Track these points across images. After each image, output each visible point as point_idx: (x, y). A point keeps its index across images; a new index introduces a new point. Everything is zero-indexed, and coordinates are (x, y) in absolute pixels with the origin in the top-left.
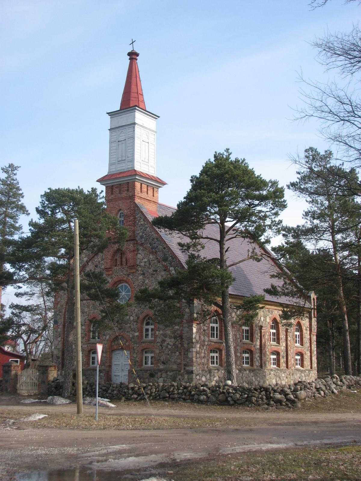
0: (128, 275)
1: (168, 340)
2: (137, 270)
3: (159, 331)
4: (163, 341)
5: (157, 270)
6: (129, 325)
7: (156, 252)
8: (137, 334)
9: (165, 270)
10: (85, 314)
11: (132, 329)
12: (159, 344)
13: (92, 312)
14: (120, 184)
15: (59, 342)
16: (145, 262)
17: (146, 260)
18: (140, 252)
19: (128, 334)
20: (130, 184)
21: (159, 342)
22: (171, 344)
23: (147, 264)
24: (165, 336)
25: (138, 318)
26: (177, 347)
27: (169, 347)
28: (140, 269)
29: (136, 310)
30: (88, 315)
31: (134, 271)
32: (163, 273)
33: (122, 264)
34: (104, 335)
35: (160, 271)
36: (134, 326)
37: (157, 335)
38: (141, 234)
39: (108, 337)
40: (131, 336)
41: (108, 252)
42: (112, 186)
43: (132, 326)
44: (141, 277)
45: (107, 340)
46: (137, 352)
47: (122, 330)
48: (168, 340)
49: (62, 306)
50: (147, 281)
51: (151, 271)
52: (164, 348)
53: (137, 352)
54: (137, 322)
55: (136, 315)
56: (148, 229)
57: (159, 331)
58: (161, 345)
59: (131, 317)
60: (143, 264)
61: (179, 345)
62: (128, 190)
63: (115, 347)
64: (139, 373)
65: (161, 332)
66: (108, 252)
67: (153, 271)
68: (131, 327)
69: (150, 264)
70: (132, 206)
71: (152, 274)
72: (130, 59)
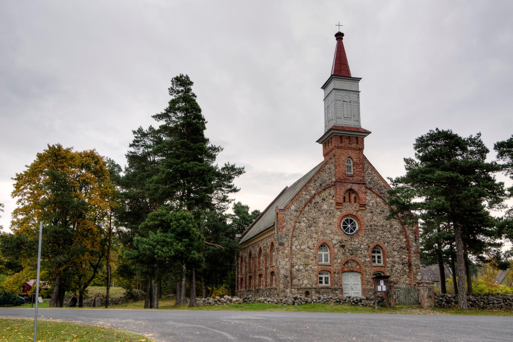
0: (357, 211)
1: (397, 266)
10: (313, 239)
12: (389, 269)
13: (321, 238)
14: (349, 137)
15: (287, 262)
16: (373, 203)
17: (373, 201)
18: (368, 194)
19: (360, 259)
20: (359, 139)
22: (400, 268)
23: (375, 205)
24: (394, 262)
25: (369, 247)
26: (405, 271)
27: (398, 271)
28: (368, 208)
31: (364, 208)
33: (350, 201)
36: (366, 253)
38: (369, 180)
39: (339, 261)
40: (363, 261)
41: (340, 190)
42: (341, 137)
44: (370, 214)
45: (339, 263)
47: (353, 256)
48: (397, 266)
49: (289, 230)
52: (394, 272)
55: (367, 244)
56: (376, 178)
60: (371, 204)
61: (407, 270)
62: (357, 143)
63: (346, 269)
66: (340, 190)
70: (361, 157)
71: (380, 213)
72: (337, 39)
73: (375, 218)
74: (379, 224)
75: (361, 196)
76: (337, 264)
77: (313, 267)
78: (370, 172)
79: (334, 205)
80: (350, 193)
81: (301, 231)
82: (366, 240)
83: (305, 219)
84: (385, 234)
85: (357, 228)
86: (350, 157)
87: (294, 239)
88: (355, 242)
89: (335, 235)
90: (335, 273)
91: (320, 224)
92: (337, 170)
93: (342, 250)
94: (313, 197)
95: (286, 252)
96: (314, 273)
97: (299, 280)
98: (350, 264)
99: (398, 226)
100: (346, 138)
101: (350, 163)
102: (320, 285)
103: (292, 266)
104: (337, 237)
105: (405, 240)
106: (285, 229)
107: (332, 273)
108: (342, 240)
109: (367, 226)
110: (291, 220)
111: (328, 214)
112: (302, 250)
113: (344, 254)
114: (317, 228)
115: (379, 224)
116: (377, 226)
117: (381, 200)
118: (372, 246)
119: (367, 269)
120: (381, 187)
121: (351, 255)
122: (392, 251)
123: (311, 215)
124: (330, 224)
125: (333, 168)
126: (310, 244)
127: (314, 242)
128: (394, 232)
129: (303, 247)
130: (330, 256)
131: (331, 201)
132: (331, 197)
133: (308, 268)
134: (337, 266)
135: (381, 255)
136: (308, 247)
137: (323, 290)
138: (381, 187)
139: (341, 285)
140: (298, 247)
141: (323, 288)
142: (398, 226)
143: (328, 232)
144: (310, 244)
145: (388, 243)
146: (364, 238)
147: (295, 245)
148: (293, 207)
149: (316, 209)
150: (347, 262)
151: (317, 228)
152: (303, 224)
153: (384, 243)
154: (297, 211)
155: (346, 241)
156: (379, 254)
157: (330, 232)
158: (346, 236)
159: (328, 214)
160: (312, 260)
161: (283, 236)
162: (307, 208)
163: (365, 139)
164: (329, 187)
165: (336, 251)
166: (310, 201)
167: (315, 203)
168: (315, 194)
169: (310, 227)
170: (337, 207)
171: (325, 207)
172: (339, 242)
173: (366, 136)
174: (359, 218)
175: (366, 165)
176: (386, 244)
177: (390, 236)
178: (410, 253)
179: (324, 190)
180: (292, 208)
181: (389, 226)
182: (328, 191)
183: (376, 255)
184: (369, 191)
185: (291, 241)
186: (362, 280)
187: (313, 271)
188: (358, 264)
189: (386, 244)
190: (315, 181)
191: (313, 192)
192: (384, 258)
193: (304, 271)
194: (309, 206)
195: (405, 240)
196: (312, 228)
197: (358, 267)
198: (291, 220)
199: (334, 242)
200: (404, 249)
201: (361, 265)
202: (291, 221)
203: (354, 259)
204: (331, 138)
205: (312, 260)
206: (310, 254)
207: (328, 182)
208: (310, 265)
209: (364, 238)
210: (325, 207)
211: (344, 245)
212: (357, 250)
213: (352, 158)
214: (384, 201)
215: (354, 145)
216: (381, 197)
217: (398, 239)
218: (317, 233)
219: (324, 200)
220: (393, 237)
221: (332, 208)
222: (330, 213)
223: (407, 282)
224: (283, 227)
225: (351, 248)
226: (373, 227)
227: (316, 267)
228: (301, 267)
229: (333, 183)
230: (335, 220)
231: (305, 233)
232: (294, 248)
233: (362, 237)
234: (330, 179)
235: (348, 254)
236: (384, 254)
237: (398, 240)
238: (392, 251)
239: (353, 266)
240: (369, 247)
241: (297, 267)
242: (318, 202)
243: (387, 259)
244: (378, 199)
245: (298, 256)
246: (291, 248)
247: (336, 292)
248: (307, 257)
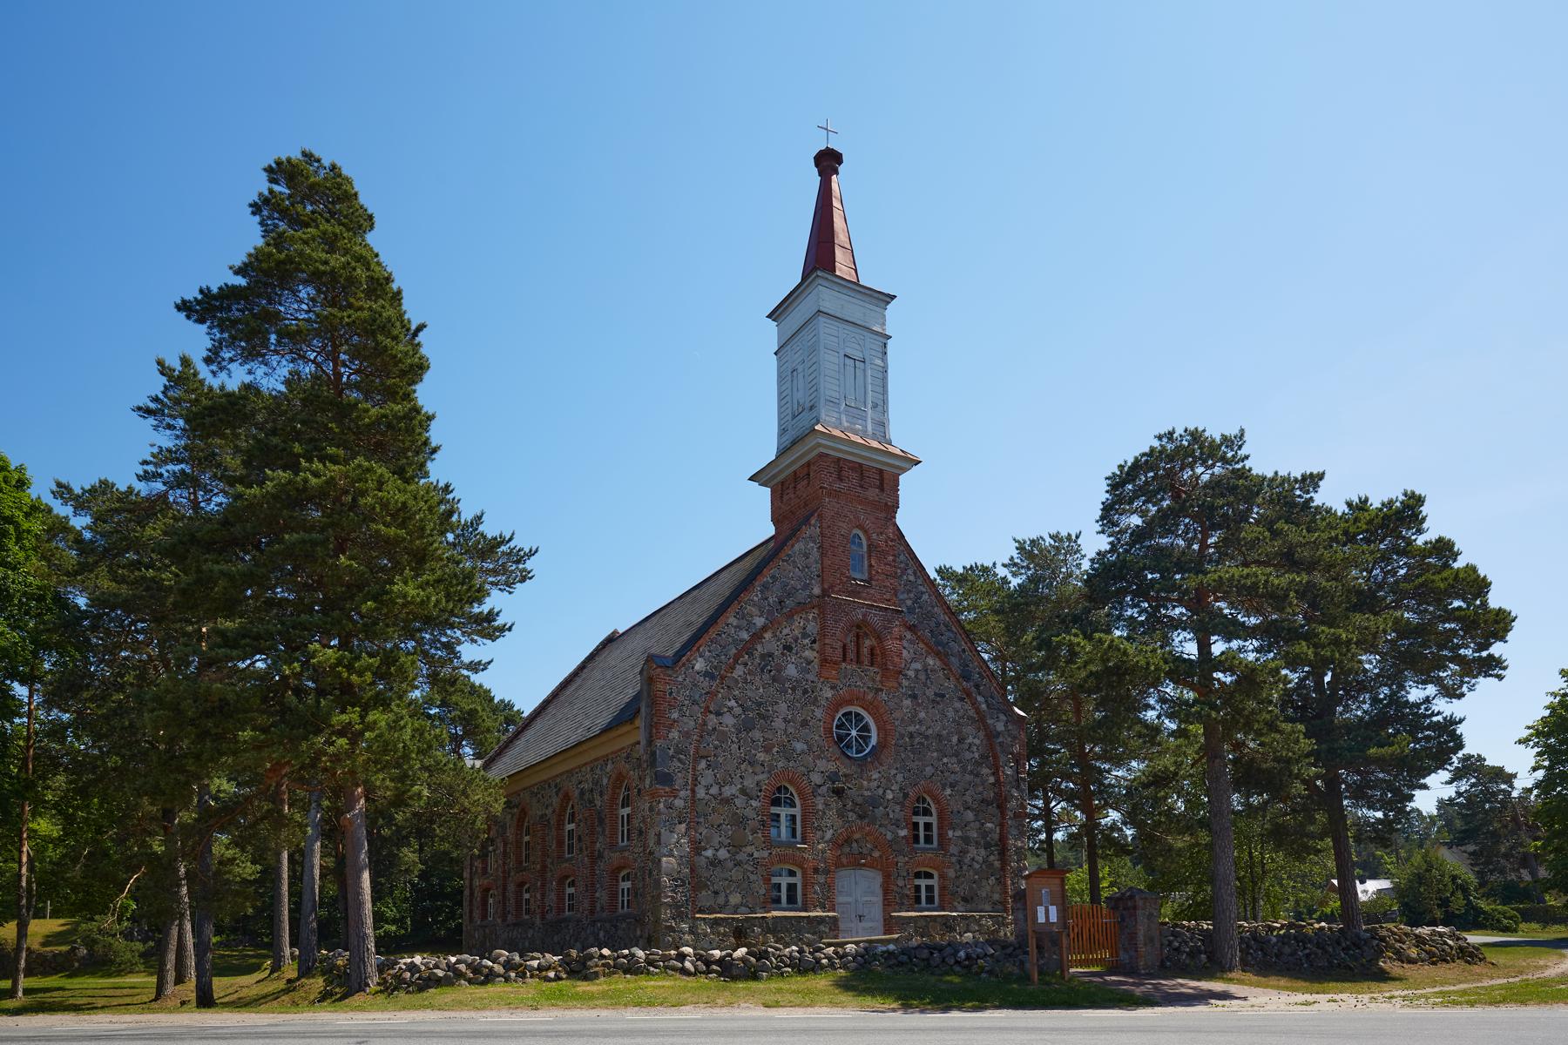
1: (973, 852)
2: (900, 684)
4: (963, 852)
5: (943, 696)
7: (947, 655)
8: (903, 833)
9: (962, 699)
12: (954, 859)
13: (780, 764)
16: (917, 671)
17: (918, 666)
23: (922, 677)
24: (966, 840)
25: (906, 796)
29: (900, 778)
32: (958, 705)
33: (859, 661)
34: (819, 828)
35: (951, 699)
36: (896, 812)
40: (889, 836)
42: (839, 459)
44: (908, 702)
48: (973, 852)
49: (687, 735)
50: (922, 715)
51: (930, 693)
54: (902, 804)
56: (925, 597)
60: (911, 673)
61: (997, 864)
65: (958, 833)
69: (928, 678)
73: (922, 715)
74: (930, 732)
75: (891, 645)
78: (912, 578)
79: (816, 664)
80: (858, 636)
81: (723, 737)
83: (733, 703)
85: (874, 741)
86: (861, 527)
87: (703, 764)
88: (870, 780)
89: (819, 757)
91: (778, 723)
92: (827, 562)
93: (835, 803)
94: (757, 636)
95: (679, 803)
97: (716, 893)
98: (855, 845)
99: (977, 742)
100: (852, 469)
101: (860, 545)
103: (697, 848)
104: (821, 765)
105: (992, 779)
106: (674, 734)
107: (810, 872)
108: (836, 774)
109: (902, 736)
110: (694, 702)
111: (799, 692)
112: (727, 801)
113: (841, 815)
115: (930, 732)
116: (927, 737)
120: (938, 624)
124: (805, 723)
125: (815, 554)
127: (761, 777)
128: (968, 755)
129: (728, 791)
130: (803, 821)
131: (807, 653)
132: (807, 641)
133: (742, 856)
138: (938, 624)
140: (714, 790)
142: (977, 742)
143: (799, 746)
144: (749, 783)
145: (952, 786)
147: (703, 783)
148: (699, 665)
149: (766, 676)
150: (848, 841)
152: (729, 720)
154: (712, 677)
156: (927, 819)
160: (754, 832)
161: (671, 752)
162: (739, 671)
163: (901, 478)
164: (802, 607)
166: (748, 648)
167: (763, 656)
168: (764, 629)
169: (749, 729)
171: (791, 671)
173: (905, 470)
175: (902, 558)
176: (948, 791)
178: (1003, 814)
179: (790, 616)
180: (697, 667)
181: (955, 739)
182: (798, 622)
183: (922, 820)
184: (909, 635)
185: (694, 769)
186: (886, 892)
187: (757, 863)
189: (948, 791)
190: (765, 587)
191: (760, 622)
192: (940, 828)
193: (730, 864)
195: (992, 779)
196: (756, 734)
198: (694, 702)
199: (816, 778)
200: (989, 803)
202: (696, 707)
204: (808, 464)
205: (754, 832)
206: (749, 813)
207: (802, 596)
208: (749, 849)
209: (893, 772)
210: (791, 671)
212: (874, 802)
213: (866, 532)
214: (946, 665)
215: (872, 493)
216: (937, 654)
217: (977, 775)
218: (767, 750)
219: (788, 648)
220: (964, 769)
221: (811, 677)
222: (805, 692)
223: (996, 897)
224: (671, 726)
225: (859, 800)
227: (765, 854)
228: (723, 854)
229: (815, 601)
232: (701, 793)
234: (806, 587)
235: (852, 816)
236: (940, 818)
237: (978, 780)
240: (906, 796)
241: (709, 853)
242: (771, 655)
243: (950, 833)
245: (716, 819)
246: (693, 791)
248: (740, 821)
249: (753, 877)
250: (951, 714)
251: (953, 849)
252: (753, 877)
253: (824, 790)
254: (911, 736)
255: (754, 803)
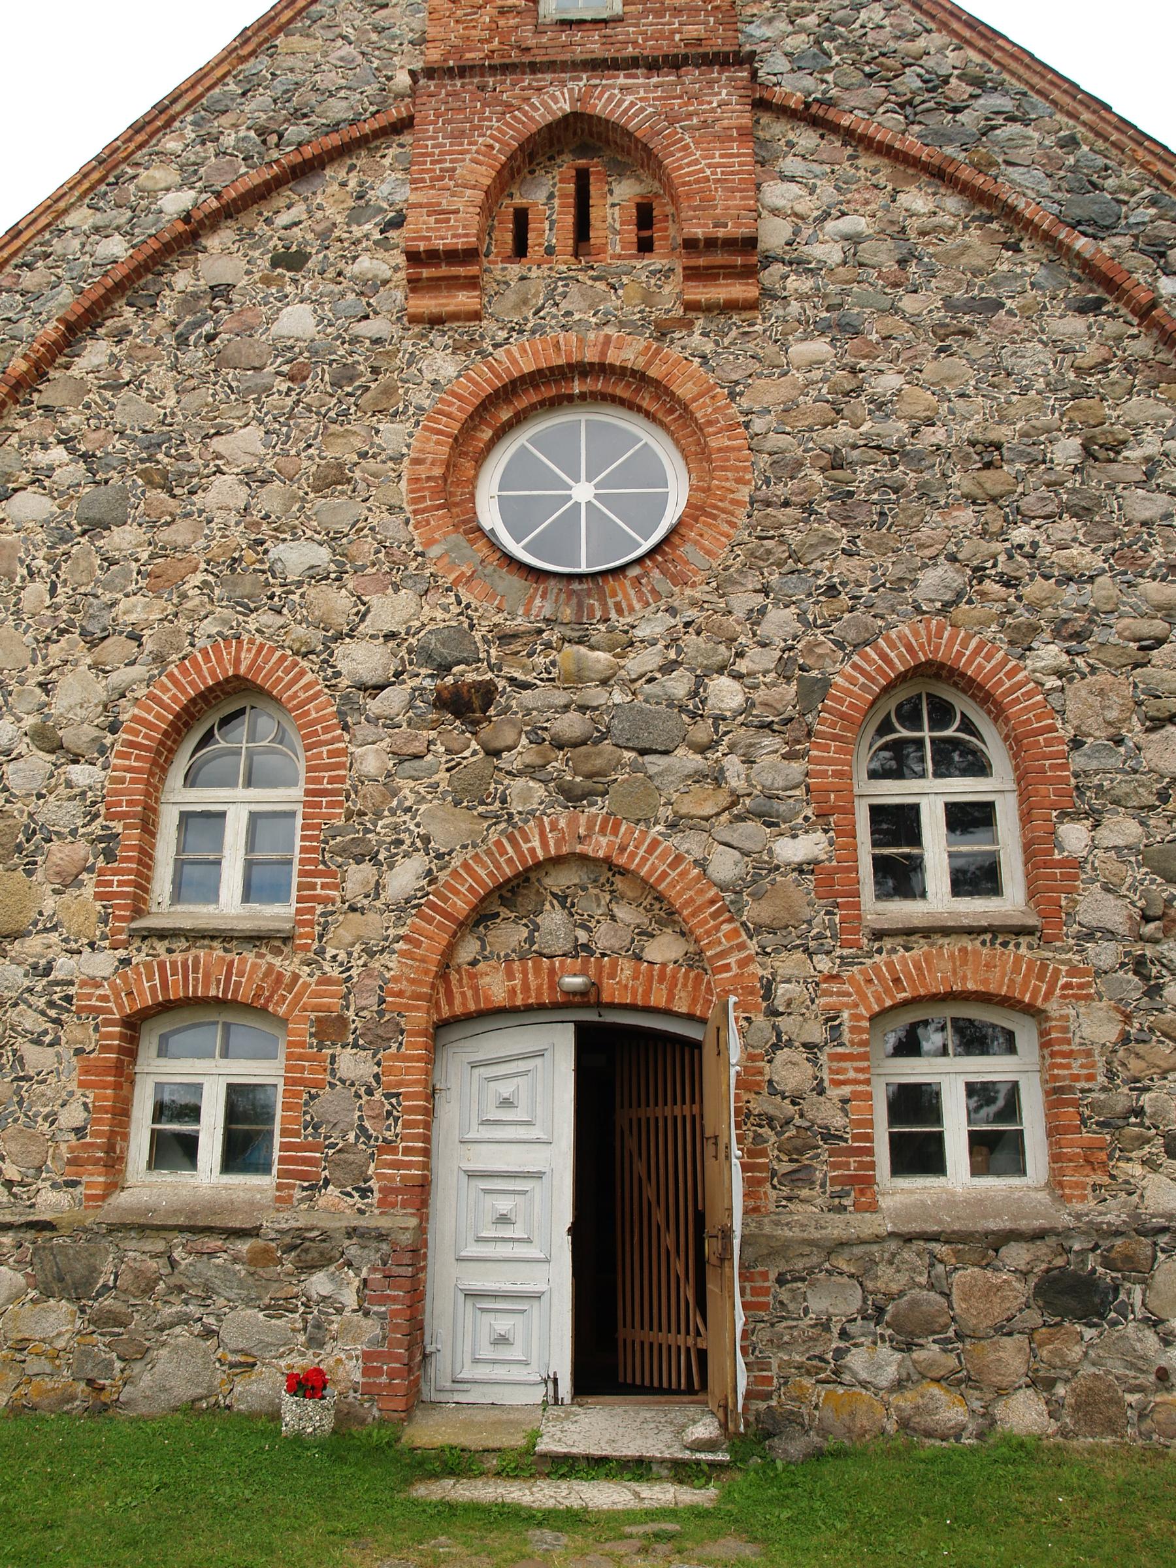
0: (662, 332)
3: (1096, 819)
6: (687, 760)
10: (116, 647)
11: (736, 799)
12: (1105, 954)
13: (209, 627)
17: (857, 223)
19: (691, 844)
21: (1111, 935)
23: (884, 255)
30: (159, 659)
37: (1078, 864)
39: (404, 877)
40: (725, 866)
43: (733, 764)
45: (403, 908)
46: (816, 1032)
47: (597, 809)
53: (816, 1032)
54: (793, 730)
55: (785, 669)
57: (1096, 819)
58: (1139, 965)
59: (723, 682)
63: (497, 987)
64: (888, 1279)
65: (1123, 829)
67: (949, 304)
68: (718, 778)
71: (941, 332)
74: (935, 435)
76: (375, 924)
77: (65, 965)
82: (780, 621)
84: (1021, 534)
90: (331, 1029)
91: (224, 492)
93: (449, 745)
96: (76, 1032)
98: (553, 919)
102: (147, 1187)
104: (392, 609)
108: (462, 635)
114: (179, 533)
115: (935, 435)
116: (915, 460)
117: (953, 203)
118: (852, 680)
119: (790, 963)
121: (573, 797)
122: (1134, 732)
123: (131, 410)
124: (334, 479)
126: (77, 696)
127: (123, 676)
131: (365, 264)
134: (374, 938)
135: (996, 786)
136: (47, 739)
137: (140, 1254)
139: (420, 1193)
141: (144, 1229)
143: (297, 556)
146: (744, 600)
150: (514, 892)
151: (179, 533)
153: (1022, 641)
155: (506, 638)
156: (966, 788)
157: (323, 555)
158: (513, 582)
159: (317, 386)
165: (371, 759)
167: (190, 301)
169: (95, 526)
170: (428, 304)
171: (297, 321)
172: (425, 655)
174: (684, 390)
176: (1049, 654)
177: (1085, 558)
181: (1067, 450)
183: (931, 795)
187: (63, 1005)
188: (666, 914)
189: (1049, 654)
192: (1026, 818)
194: (120, 336)
197: (664, 949)
199: (362, 659)
201: (702, 922)
203: (600, 845)
205: (69, 881)
206: (59, 812)
208: (34, 944)
209: (744, 600)
211: (487, 692)
218: (158, 581)
225: (571, 725)
226: (865, 474)
227: (102, 964)
230: (393, 434)
231: (38, 588)
233: (723, 585)
238: (1134, 732)
239: (604, 937)
240: (815, 691)
242: (221, 291)
243: (1074, 836)
244: (917, 200)
247: (319, 1283)
249: (37, 1058)
250: (1034, 359)
251: (1098, 908)
252: (37, 1058)
253: (393, 700)
254: (836, 461)
255: (81, 774)
